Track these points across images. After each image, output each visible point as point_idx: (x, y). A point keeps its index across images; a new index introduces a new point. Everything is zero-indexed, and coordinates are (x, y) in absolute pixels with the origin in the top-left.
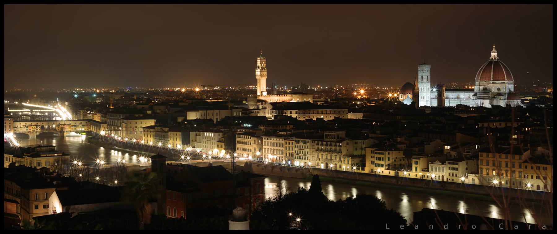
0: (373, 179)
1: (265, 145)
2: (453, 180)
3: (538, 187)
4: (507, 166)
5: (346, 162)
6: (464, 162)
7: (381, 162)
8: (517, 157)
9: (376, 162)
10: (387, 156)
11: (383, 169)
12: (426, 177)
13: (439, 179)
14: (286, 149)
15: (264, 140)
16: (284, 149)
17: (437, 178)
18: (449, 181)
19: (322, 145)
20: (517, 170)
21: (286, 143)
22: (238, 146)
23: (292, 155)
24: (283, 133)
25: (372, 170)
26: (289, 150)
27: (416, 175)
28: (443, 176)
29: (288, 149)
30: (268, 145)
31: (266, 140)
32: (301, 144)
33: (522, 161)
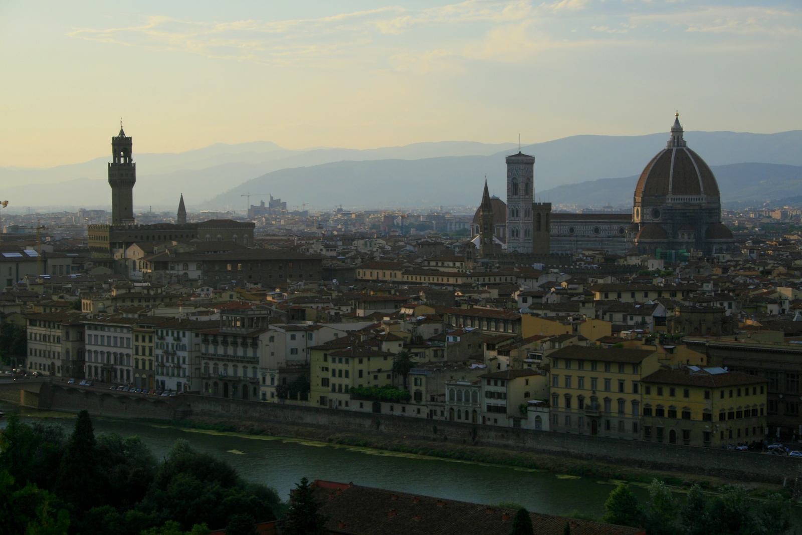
0: (323, 420)
1: (90, 344)
2: (496, 421)
3: (672, 433)
4: (607, 388)
8: (629, 370)
10: (359, 367)
11: (345, 397)
12: (439, 413)
13: (467, 418)
14: (137, 353)
15: (87, 332)
16: (131, 352)
17: (463, 415)
18: (488, 423)
20: (629, 397)
21: (137, 340)
22: (32, 345)
24: (130, 316)
25: (323, 400)
26: (144, 354)
27: (419, 411)
28: (475, 411)
29: (140, 352)
30: (96, 344)
31: (93, 332)
32: (170, 339)
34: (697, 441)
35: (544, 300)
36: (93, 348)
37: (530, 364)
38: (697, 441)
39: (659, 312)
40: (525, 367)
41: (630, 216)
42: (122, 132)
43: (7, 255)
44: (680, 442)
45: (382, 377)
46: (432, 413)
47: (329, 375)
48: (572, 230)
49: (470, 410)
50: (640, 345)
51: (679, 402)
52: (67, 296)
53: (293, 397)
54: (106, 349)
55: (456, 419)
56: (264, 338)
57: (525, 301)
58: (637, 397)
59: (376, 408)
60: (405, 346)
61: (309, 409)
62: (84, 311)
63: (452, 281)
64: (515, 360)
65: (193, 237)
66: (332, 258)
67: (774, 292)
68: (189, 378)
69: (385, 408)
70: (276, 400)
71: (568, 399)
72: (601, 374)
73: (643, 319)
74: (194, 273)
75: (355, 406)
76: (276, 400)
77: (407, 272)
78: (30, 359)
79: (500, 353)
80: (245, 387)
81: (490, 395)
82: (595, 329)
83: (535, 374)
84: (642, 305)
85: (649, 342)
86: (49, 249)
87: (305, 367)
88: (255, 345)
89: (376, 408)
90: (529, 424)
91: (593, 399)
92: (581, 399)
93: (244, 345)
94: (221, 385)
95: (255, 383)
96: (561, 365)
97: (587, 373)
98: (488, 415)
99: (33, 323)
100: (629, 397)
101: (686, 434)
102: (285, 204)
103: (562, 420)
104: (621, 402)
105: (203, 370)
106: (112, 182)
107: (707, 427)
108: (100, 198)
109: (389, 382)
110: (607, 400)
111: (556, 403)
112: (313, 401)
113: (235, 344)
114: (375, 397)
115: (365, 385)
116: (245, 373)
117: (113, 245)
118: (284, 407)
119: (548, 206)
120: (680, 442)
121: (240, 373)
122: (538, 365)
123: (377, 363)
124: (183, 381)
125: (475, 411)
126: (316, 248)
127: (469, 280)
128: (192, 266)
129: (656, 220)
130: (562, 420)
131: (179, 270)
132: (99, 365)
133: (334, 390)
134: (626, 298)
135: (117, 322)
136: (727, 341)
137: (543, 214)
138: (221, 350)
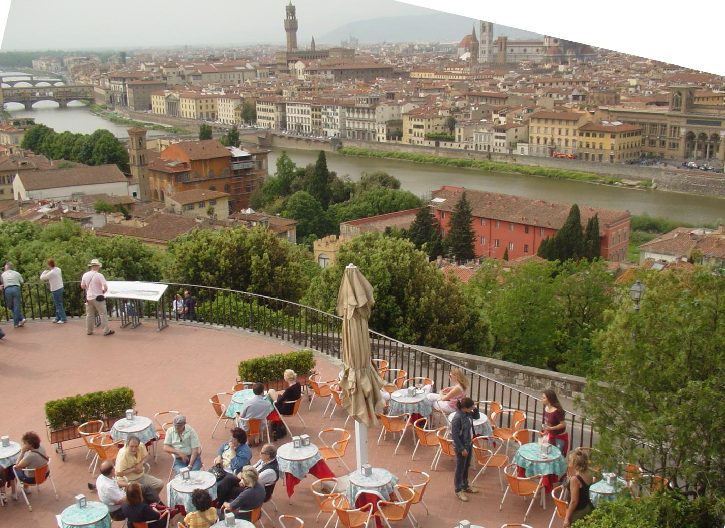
0: (410, 151)
3: (593, 156)
5: (381, 131)
6: (514, 129)
7: (421, 131)
8: (571, 124)
9: (415, 130)
10: (428, 123)
15: (287, 107)
16: (310, 117)
17: (483, 148)
19: (353, 112)
20: (571, 137)
22: (259, 114)
23: (320, 124)
28: (489, 146)
31: (290, 107)
32: (330, 110)
33: (576, 128)
34: (606, 160)
35: (514, 87)
36: (290, 115)
37: (516, 121)
38: (606, 160)
39: (575, 93)
40: (514, 122)
41: (542, 43)
42: (290, 3)
43: (237, 68)
44: (597, 161)
45: (439, 128)
46: (466, 147)
47: (412, 128)
48: (512, 50)
49: (486, 145)
50: (577, 111)
51: (598, 140)
52: (272, 89)
53: (394, 139)
54: (297, 115)
55: (479, 150)
56: (378, 109)
57: (504, 87)
58: (575, 138)
59: (437, 144)
60: (451, 112)
61: (403, 145)
62: (284, 96)
63: (460, 78)
64: (508, 119)
65: (327, 57)
66: (396, 67)
67: (626, 81)
68: (340, 130)
69: (442, 144)
70: (385, 140)
71: (538, 140)
72: (557, 126)
73: (567, 96)
74: (330, 76)
75: (426, 143)
76: (385, 140)
77: (436, 73)
78: (259, 121)
79: (501, 115)
80: (369, 134)
81: (497, 137)
82: (548, 104)
83: (519, 126)
84: (567, 90)
85: (581, 109)
86: (257, 64)
87: (399, 123)
88: (374, 113)
89: (437, 144)
90: (517, 152)
91: (552, 140)
92: (545, 140)
93: (368, 113)
94: (356, 133)
95: (375, 133)
96: (536, 121)
97: (549, 125)
98: (495, 148)
99: (259, 102)
100: (571, 137)
101: (601, 157)
102: (357, 40)
103: (535, 149)
104: (567, 141)
105: (347, 126)
106: (287, 30)
107: (612, 153)
108: (280, 39)
109: (443, 131)
110: (559, 139)
111: (532, 142)
112: (405, 140)
113: (363, 112)
114: (437, 138)
115: (431, 133)
116: (369, 127)
117: (288, 62)
118: (390, 144)
119: (506, 38)
120: (597, 161)
121: (366, 127)
122: (521, 121)
123: (437, 121)
124: (337, 131)
125: (489, 146)
126: (388, 61)
127: (469, 77)
128: (329, 72)
129: (556, 45)
130: (535, 149)
131: (323, 75)
132: (294, 124)
133: (415, 135)
134: (554, 86)
135: (301, 102)
136: (619, 108)
137: (503, 43)
138: (356, 116)
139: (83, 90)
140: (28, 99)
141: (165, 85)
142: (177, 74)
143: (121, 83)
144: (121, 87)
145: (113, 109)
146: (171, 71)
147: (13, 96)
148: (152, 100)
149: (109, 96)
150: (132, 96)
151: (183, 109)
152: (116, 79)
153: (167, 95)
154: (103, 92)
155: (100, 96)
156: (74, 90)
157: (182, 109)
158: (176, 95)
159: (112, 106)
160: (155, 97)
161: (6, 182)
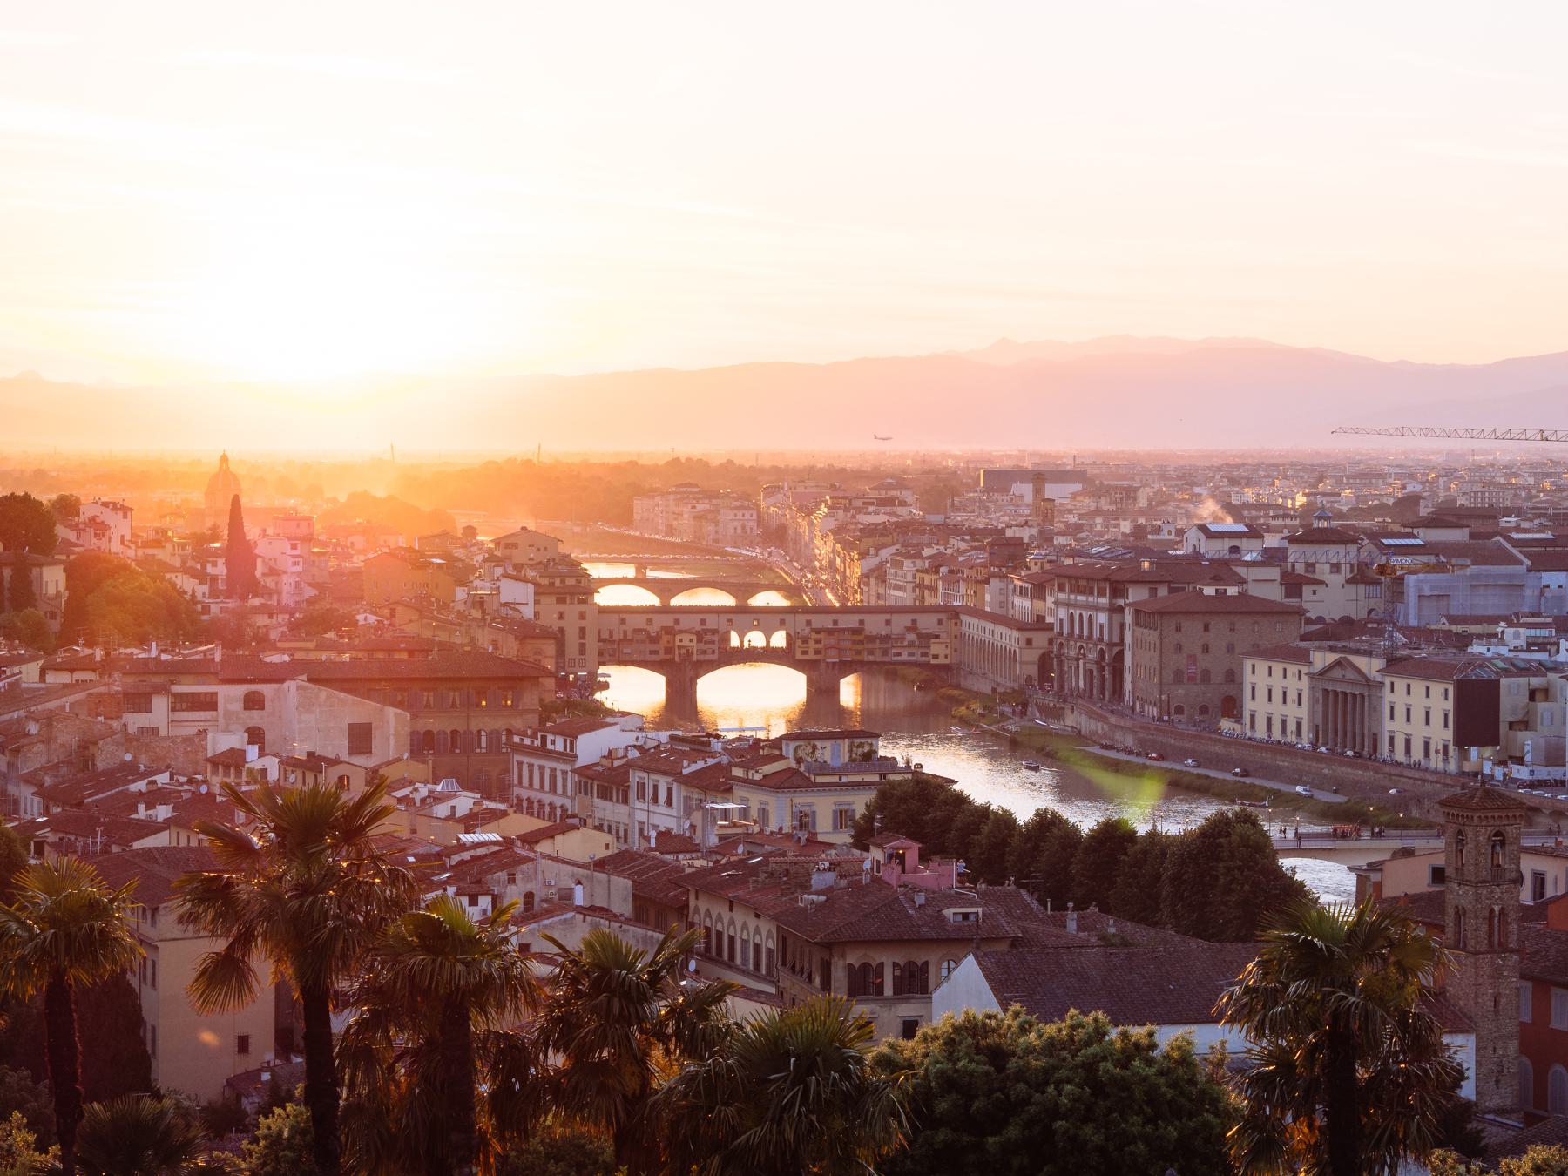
139: (913, 628)
140: (684, 650)
141: (1300, 612)
142: (1345, 572)
143: (1104, 601)
144: (1102, 618)
145: (1055, 713)
146: (1324, 558)
147: (625, 640)
148: (1248, 679)
149: (1033, 655)
150: (1150, 659)
151: (1394, 726)
152: (1080, 581)
153: (1321, 659)
154: (1008, 638)
155: (994, 653)
156: (874, 625)
157: (1388, 725)
158: (1371, 666)
159: (1051, 700)
160: (1262, 666)
161: (888, 991)
